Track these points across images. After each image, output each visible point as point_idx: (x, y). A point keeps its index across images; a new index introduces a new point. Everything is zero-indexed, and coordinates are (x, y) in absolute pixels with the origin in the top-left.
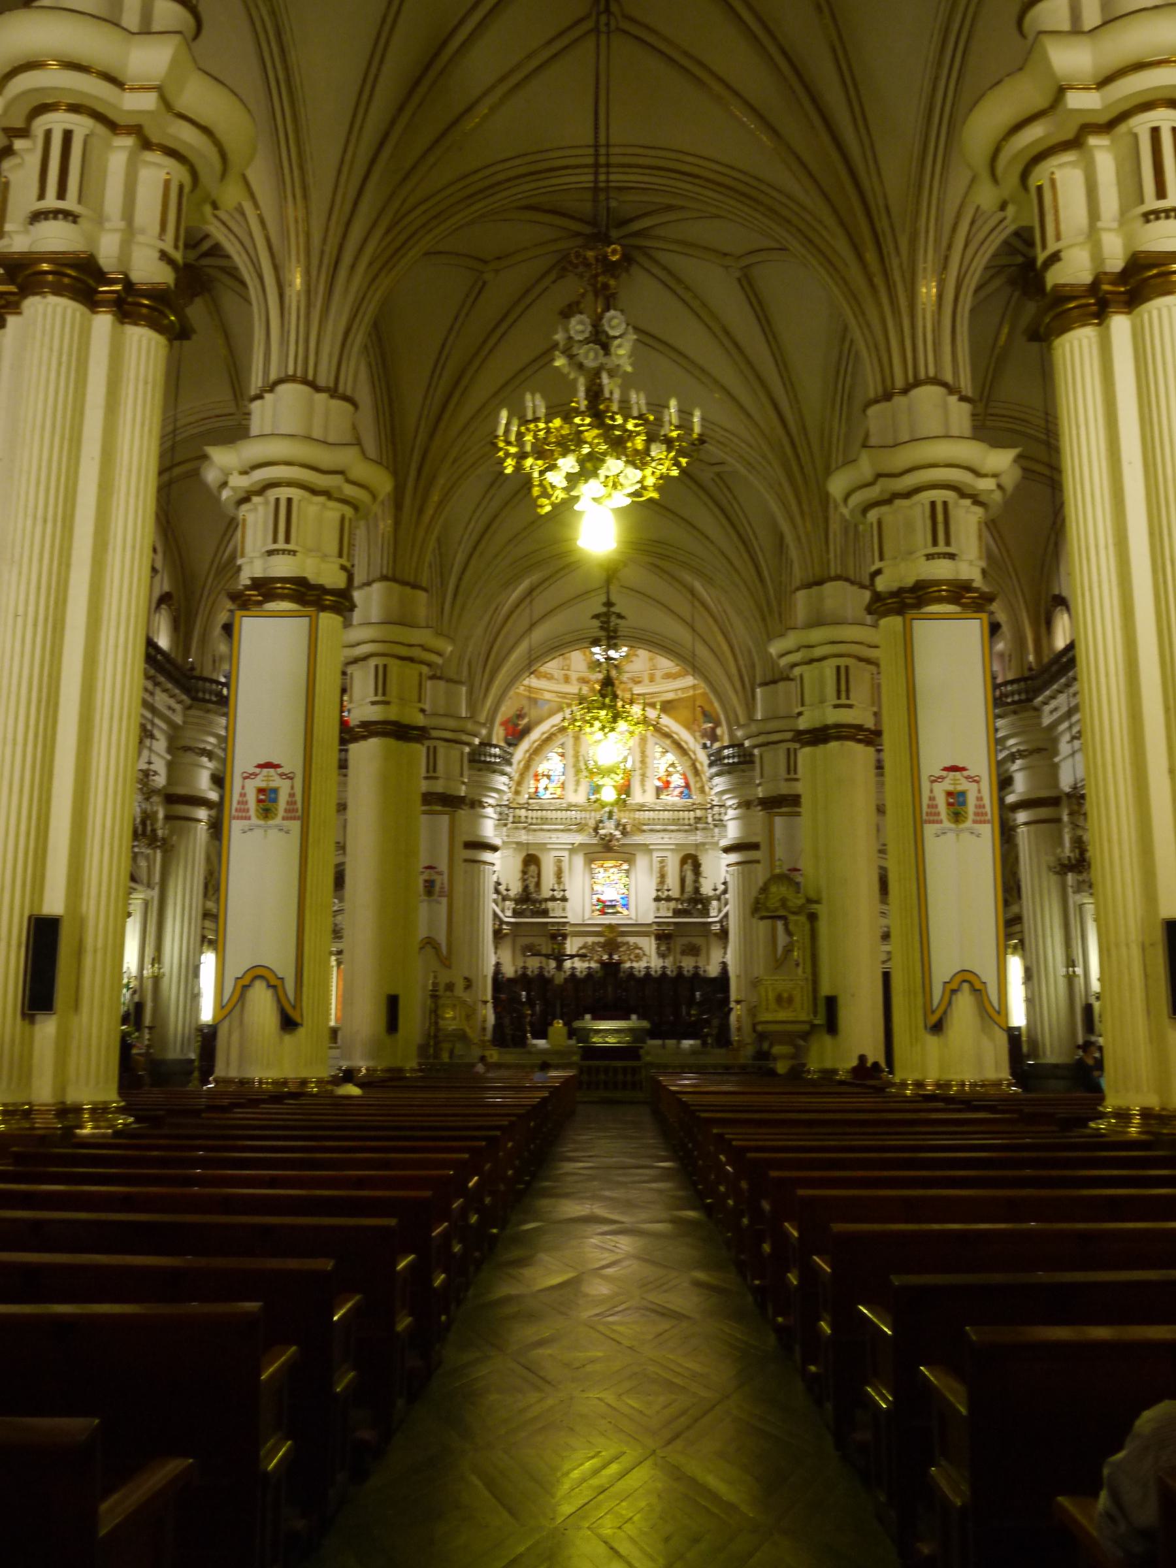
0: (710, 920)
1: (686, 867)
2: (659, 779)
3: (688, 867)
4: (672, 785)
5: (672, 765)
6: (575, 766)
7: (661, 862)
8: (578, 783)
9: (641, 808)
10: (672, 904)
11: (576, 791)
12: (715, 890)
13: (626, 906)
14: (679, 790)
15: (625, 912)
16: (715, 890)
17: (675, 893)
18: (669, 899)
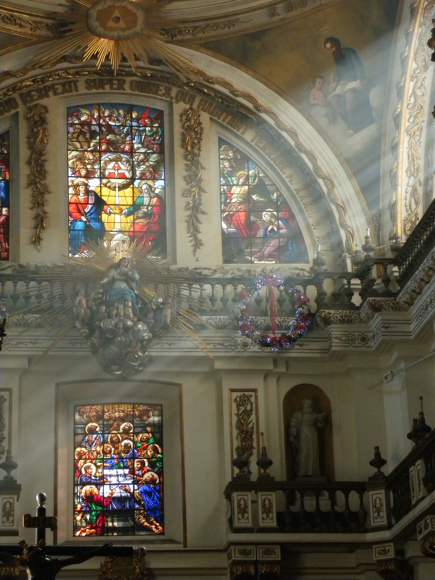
0: (370, 537)
1: (298, 415)
2: (228, 219)
3: (305, 417)
4: (261, 233)
5: (260, 187)
6: (32, 183)
7: (242, 402)
8: (40, 222)
9: (197, 277)
10: (274, 498)
11: (37, 240)
12: (378, 461)
13: (157, 512)
14: (274, 243)
15: (156, 528)
16: (378, 461)
17: (278, 470)
18: (266, 484)
